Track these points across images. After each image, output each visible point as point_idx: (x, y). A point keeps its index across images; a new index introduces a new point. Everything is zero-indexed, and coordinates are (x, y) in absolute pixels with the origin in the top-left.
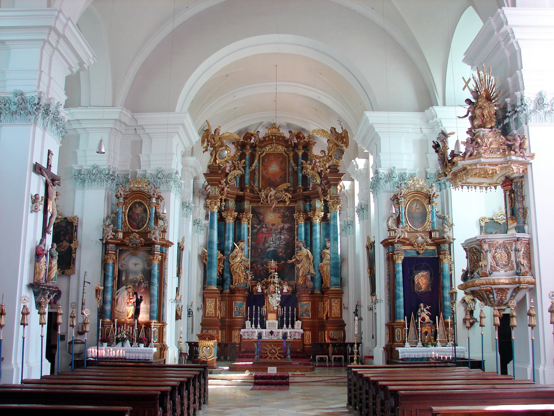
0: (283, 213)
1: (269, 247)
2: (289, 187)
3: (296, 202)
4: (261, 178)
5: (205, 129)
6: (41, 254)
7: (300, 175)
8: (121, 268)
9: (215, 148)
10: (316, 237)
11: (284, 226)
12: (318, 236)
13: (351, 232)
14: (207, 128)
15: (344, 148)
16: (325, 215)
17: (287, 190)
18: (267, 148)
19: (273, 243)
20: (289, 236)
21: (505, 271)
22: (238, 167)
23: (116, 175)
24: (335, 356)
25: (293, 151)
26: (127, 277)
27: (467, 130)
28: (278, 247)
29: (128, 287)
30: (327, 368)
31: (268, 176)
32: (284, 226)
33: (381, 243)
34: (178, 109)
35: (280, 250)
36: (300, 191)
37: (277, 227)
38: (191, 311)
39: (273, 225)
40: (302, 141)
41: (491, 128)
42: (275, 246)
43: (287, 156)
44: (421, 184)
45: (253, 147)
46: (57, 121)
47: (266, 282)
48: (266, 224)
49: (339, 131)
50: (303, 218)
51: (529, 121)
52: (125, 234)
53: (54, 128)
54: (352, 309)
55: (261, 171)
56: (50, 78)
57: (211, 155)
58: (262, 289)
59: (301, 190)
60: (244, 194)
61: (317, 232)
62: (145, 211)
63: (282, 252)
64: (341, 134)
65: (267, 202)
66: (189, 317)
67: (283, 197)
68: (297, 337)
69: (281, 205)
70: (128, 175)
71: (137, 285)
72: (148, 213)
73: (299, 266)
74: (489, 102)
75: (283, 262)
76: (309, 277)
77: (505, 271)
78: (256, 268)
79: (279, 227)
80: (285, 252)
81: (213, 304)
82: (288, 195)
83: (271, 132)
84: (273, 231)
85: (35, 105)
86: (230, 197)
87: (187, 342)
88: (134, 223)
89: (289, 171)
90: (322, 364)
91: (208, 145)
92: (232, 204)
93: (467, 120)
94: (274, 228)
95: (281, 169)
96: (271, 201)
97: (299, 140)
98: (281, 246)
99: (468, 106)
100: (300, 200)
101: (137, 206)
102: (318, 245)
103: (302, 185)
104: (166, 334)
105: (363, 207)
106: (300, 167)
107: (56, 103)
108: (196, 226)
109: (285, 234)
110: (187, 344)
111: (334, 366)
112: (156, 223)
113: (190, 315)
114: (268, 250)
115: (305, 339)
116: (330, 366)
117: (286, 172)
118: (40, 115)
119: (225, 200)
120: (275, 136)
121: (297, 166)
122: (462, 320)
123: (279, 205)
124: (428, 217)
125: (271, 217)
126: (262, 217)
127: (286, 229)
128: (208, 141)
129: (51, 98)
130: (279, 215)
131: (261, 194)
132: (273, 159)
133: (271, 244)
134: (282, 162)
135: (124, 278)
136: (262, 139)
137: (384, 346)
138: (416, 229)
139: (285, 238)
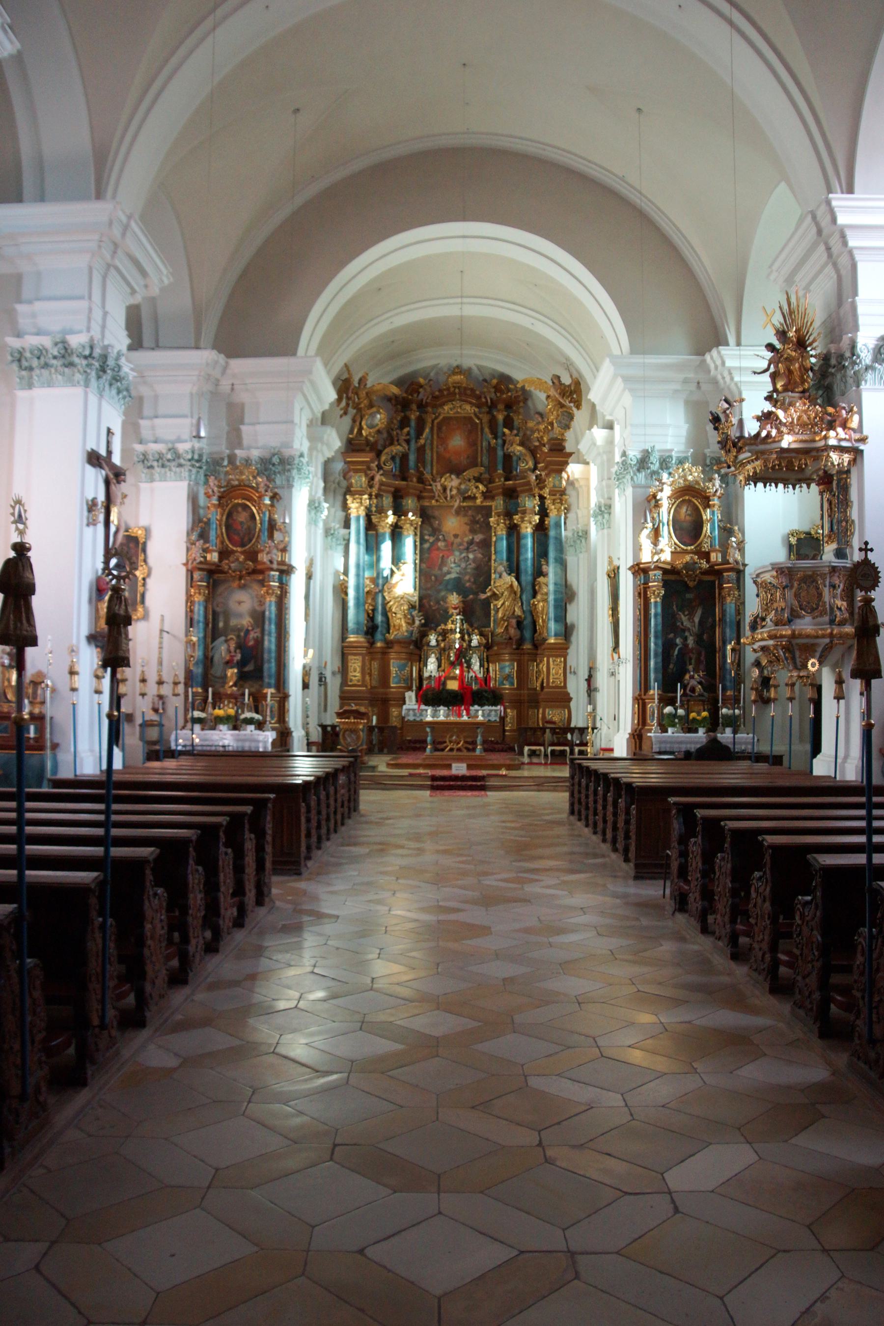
1: (449, 573)
2: (481, 474)
3: (492, 498)
4: (435, 457)
5: (344, 377)
6: (104, 590)
7: (500, 453)
8: (218, 609)
9: (359, 410)
12: (529, 555)
13: (583, 550)
14: (345, 376)
15: (575, 409)
16: (542, 521)
17: (478, 480)
18: (446, 408)
21: (814, 618)
22: (398, 440)
23: (204, 460)
25: (488, 413)
26: (226, 623)
27: (766, 394)
28: (464, 572)
29: (229, 637)
30: (543, 767)
33: (630, 569)
34: (301, 351)
35: (467, 578)
36: (500, 481)
39: (456, 536)
40: (504, 396)
41: (804, 392)
44: (696, 474)
45: (421, 406)
46: (117, 381)
47: (444, 630)
49: (566, 380)
50: (505, 523)
51: (863, 383)
52: (224, 554)
53: (114, 392)
54: (583, 674)
55: (435, 446)
56: (105, 314)
57: (354, 421)
58: (437, 641)
59: (502, 479)
60: (407, 485)
62: (253, 517)
63: (469, 581)
64: (569, 386)
65: (446, 498)
68: (493, 718)
69: (470, 504)
70: (223, 459)
71: (242, 634)
72: (258, 521)
74: (802, 349)
75: (471, 596)
76: (514, 622)
77: (814, 618)
78: (427, 606)
79: (466, 539)
82: (481, 487)
84: (455, 546)
85: (86, 357)
86: (384, 491)
87: (320, 726)
88: (236, 537)
89: (482, 447)
90: (535, 760)
91: (348, 405)
92: (388, 500)
93: (766, 378)
94: (458, 540)
96: (452, 497)
97: (498, 394)
98: (469, 570)
99: (769, 355)
100: (498, 495)
101: (240, 509)
102: (530, 570)
103: (504, 470)
104: (288, 711)
105: (603, 509)
106: (500, 441)
107: (115, 351)
108: (330, 538)
110: (320, 729)
111: (551, 764)
112: (271, 536)
114: (448, 577)
116: (546, 764)
117: (477, 450)
118: (93, 374)
119: (377, 496)
120: (459, 388)
121: (496, 440)
123: (465, 504)
124: (705, 529)
125: (452, 524)
127: (478, 543)
128: (348, 398)
129: (109, 346)
130: (466, 520)
134: (470, 432)
135: (221, 625)
136: (437, 393)
137: (629, 731)
138: (685, 548)
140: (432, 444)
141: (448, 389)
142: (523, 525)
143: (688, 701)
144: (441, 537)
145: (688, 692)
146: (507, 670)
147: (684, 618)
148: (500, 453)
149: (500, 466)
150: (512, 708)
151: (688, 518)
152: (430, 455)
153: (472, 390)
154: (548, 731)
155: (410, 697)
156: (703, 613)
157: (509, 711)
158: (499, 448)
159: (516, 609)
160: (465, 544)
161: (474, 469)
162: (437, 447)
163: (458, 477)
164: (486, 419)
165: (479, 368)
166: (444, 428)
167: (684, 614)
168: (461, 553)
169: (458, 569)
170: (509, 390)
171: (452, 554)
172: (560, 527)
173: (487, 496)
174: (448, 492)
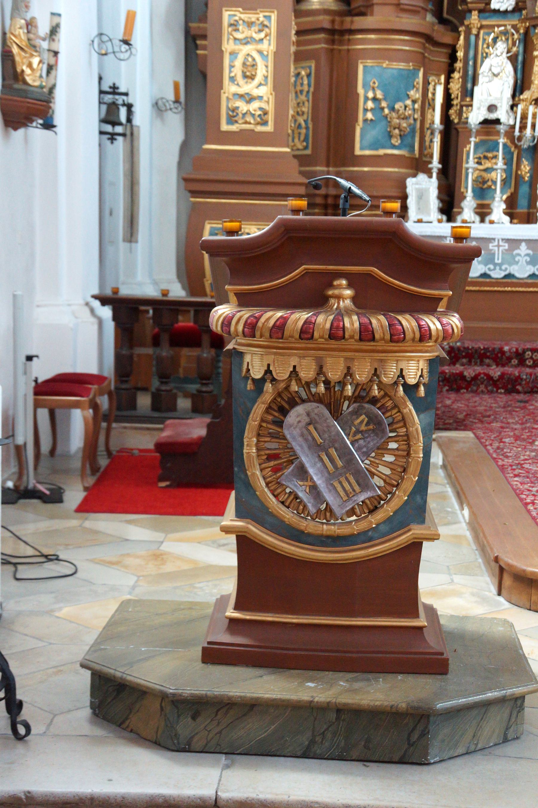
38: (120, 100)
66: (112, 137)
81: (264, 46)
87: (104, 301)
110: (106, 312)
113: (119, 129)
155: (422, 195)
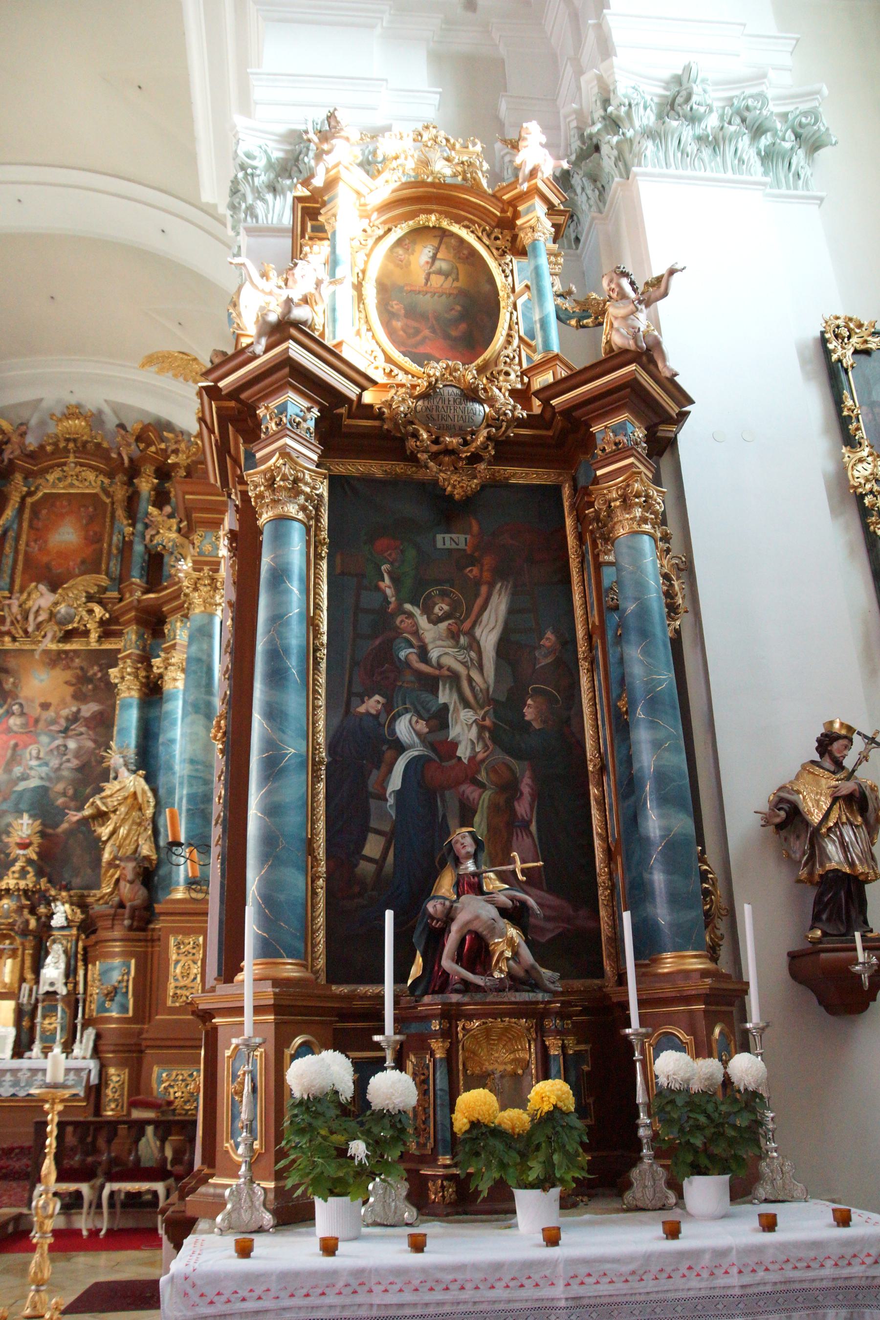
0: (82, 668)
1: (24, 778)
2: (105, 590)
3: (119, 634)
7: (139, 548)
10: (170, 735)
11: (79, 711)
18: (51, 477)
19: (39, 766)
20: (95, 741)
24: (116, 1186)
31: (45, 559)
32: (79, 711)
35: (60, 787)
37: (57, 713)
39: (45, 706)
40: (153, 449)
42: (43, 775)
43: (108, 501)
48: (21, 705)
50: (137, 676)
59: (138, 593)
61: (176, 719)
63: (64, 794)
67: (81, 618)
73: (104, 832)
76: (129, 868)
79: (65, 712)
80: (76, 791)
82: (98, 611)
83: (65, 430)
84: (41, 725)
89: (110, 545)
95: (86, 538)
96: (39, 626)
97: (142, 446)
98: (65, 773)
100: (127, 623)
109: (82, 734)
115: (107, 1096)
120: (75, 440)
121: (133, 525)
122: (784, 961)
123: (68, 647)
126: (14, 683)
127: (86, 719)
130: (68, 675)
131: (9, 606)
132: (64, 511)
133: (31, 768)
134: (91, 519)
139: (80, 748)
140: (17, 539)
141: (56, 444)
142: (169, 675)
143: (451, 1015)
144: (16, 708)
145: (447, 963)
146: (116, 976)
147: (430, 632)
148: (139, 548)
149: (136, 572)
150: (121, 1064)
151: (437, 281)
152: (11, 555)
153: (99, 445)
154: (150, 1130)
156: (511, 611)
157: (112, 1071)
158: (137, 539)
159: (141, 842)
160: (63, 722)
161: (87, 577)
162: (27, 545)
163: (53, 589)
164: (120, 493)
165: (117, 408)
166: (44, 512)
167: (427, 610)
168: (54, 739)
169: (44, 770)
170: (162, 439)
171: (37, 742)
172: (210, 636)
173: (108, 629)
174: (31, 617)
